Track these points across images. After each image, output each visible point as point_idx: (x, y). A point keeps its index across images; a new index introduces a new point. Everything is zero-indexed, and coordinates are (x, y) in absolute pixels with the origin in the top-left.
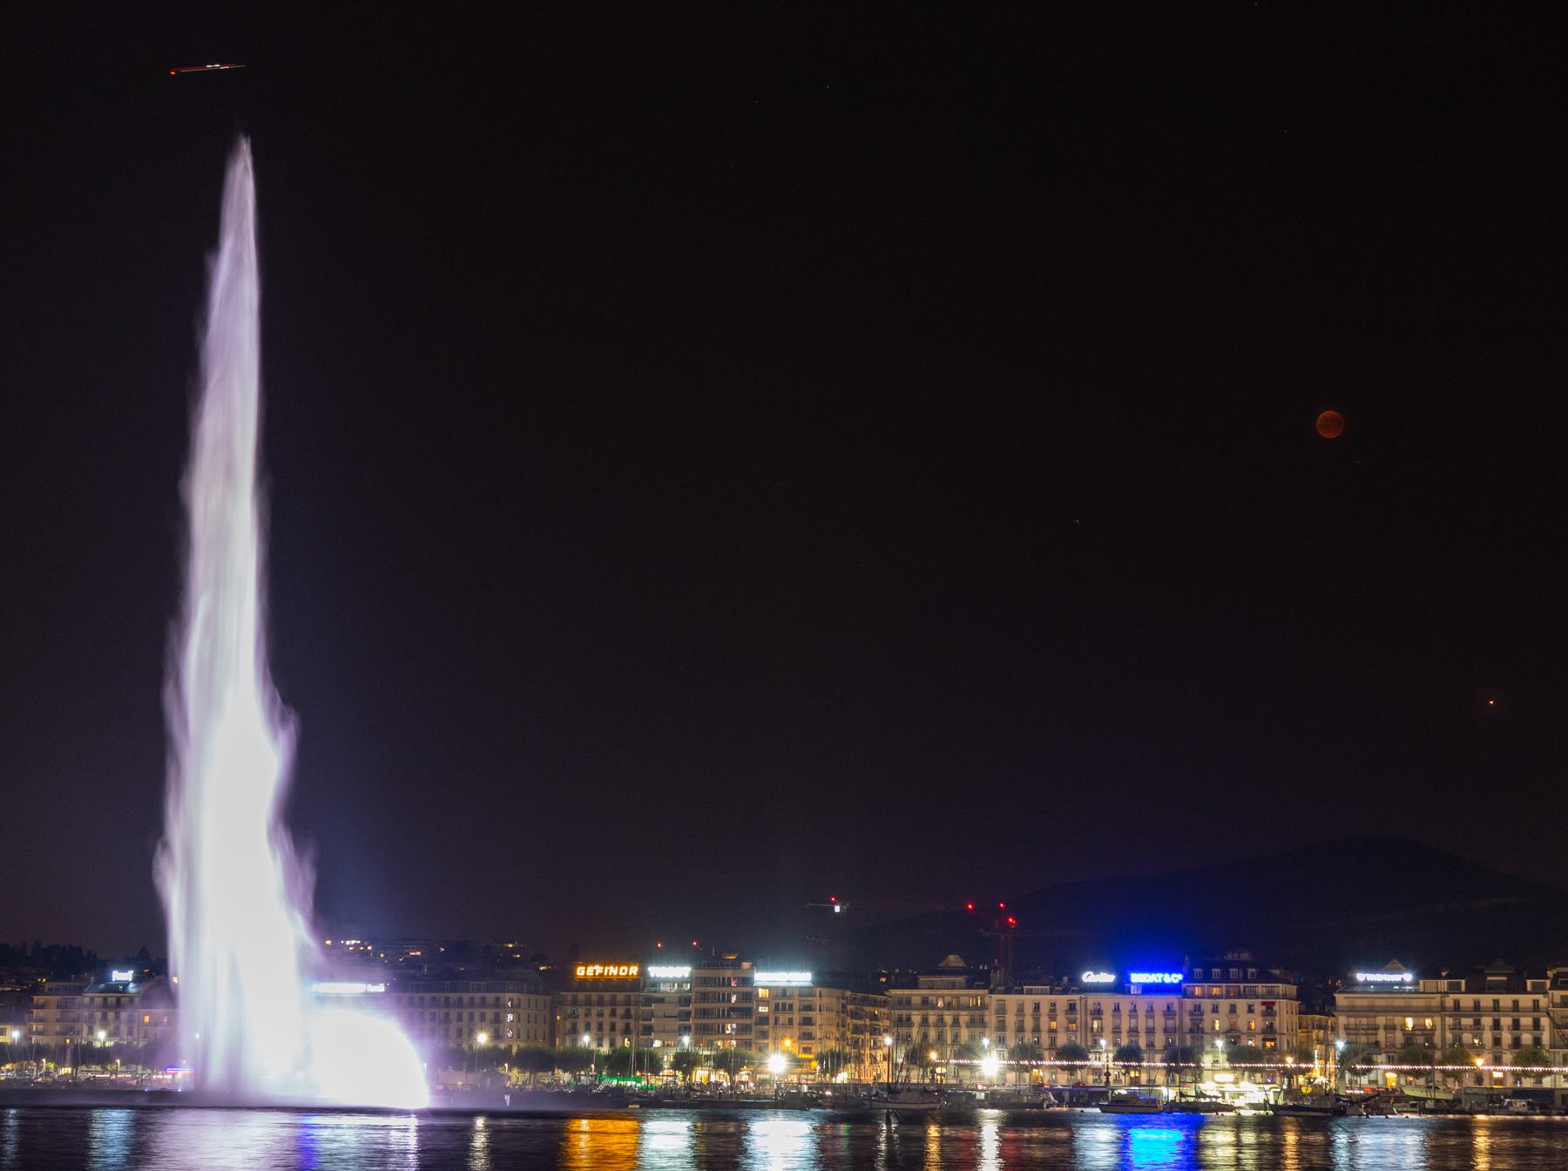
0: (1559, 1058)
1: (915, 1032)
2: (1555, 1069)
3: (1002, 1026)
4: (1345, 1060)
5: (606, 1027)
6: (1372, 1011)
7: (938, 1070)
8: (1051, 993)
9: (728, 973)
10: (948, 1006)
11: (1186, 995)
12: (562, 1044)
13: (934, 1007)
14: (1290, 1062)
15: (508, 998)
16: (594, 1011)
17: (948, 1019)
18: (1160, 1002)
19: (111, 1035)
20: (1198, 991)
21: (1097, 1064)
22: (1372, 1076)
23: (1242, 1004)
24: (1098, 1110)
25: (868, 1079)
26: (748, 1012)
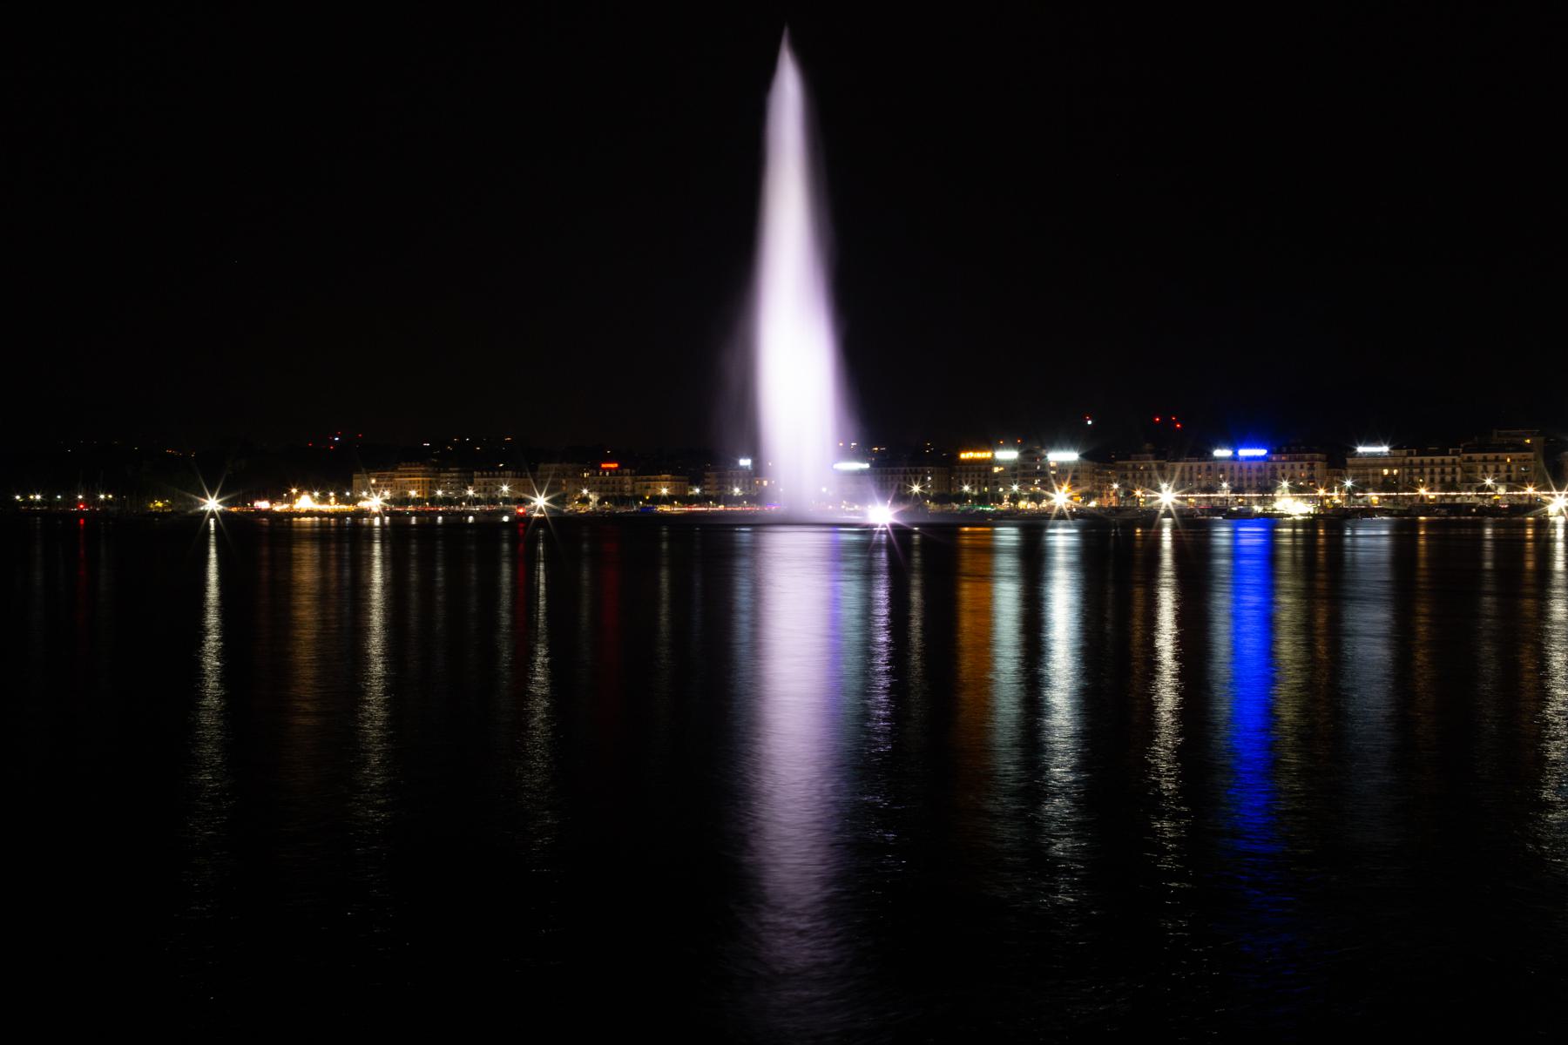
0: (1465, 488)
2: (1463, 494)
4: (1351, 492)
5: (976, 483)
6: (1365, 466)
7: (1141, 500)
8: (1199, 461)
10: (1146, 469)
12: (954, 491)
13: (1139, 469)
14: (1321, 492)
16: (970, 475)
17: (1146, 475)
20: (1274, 458)
21: (1221, 495)
22: (1365, 499)
23: (1297, 465)
24: (1221, 518)
25: (1106, 505)
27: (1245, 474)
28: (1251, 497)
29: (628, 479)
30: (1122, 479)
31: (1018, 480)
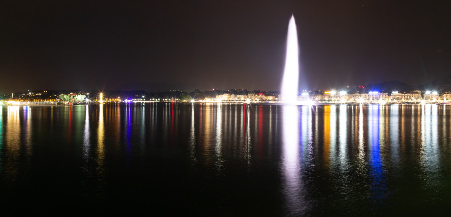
1: (355, 98)
6: (394, 96)
12: (324, 99)
17: (358, 96)
23: (383, 95)
27: (374, 97)
29: (264, 96)
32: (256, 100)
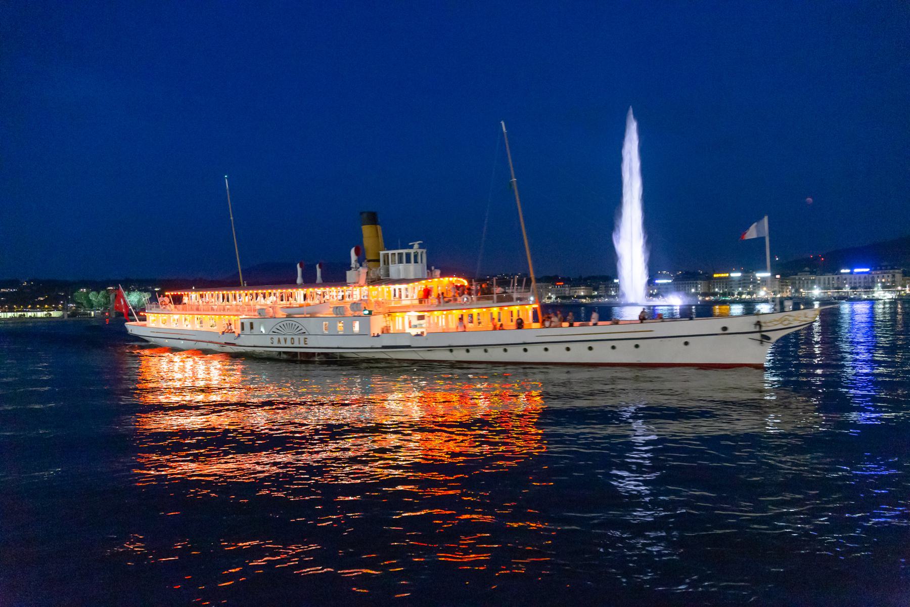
1: (797, 286)
3: (819, 283)
9: (750, 274)
10: (805, 279)
11: (870, 274)
13: (802, 280)
14: (899, 288)
15: (698, 282)
16: (719, 284)
17: (806, 282)
18: (863, 276)
19: (615, 293)
23: (886, 275)
24: (844, 301)
26: (755, 283)
27: (857, 280)
28: (861, 291)
29: (567, 289)
30: (793, 284)
31: (742, 285)
32: (550, 298)
